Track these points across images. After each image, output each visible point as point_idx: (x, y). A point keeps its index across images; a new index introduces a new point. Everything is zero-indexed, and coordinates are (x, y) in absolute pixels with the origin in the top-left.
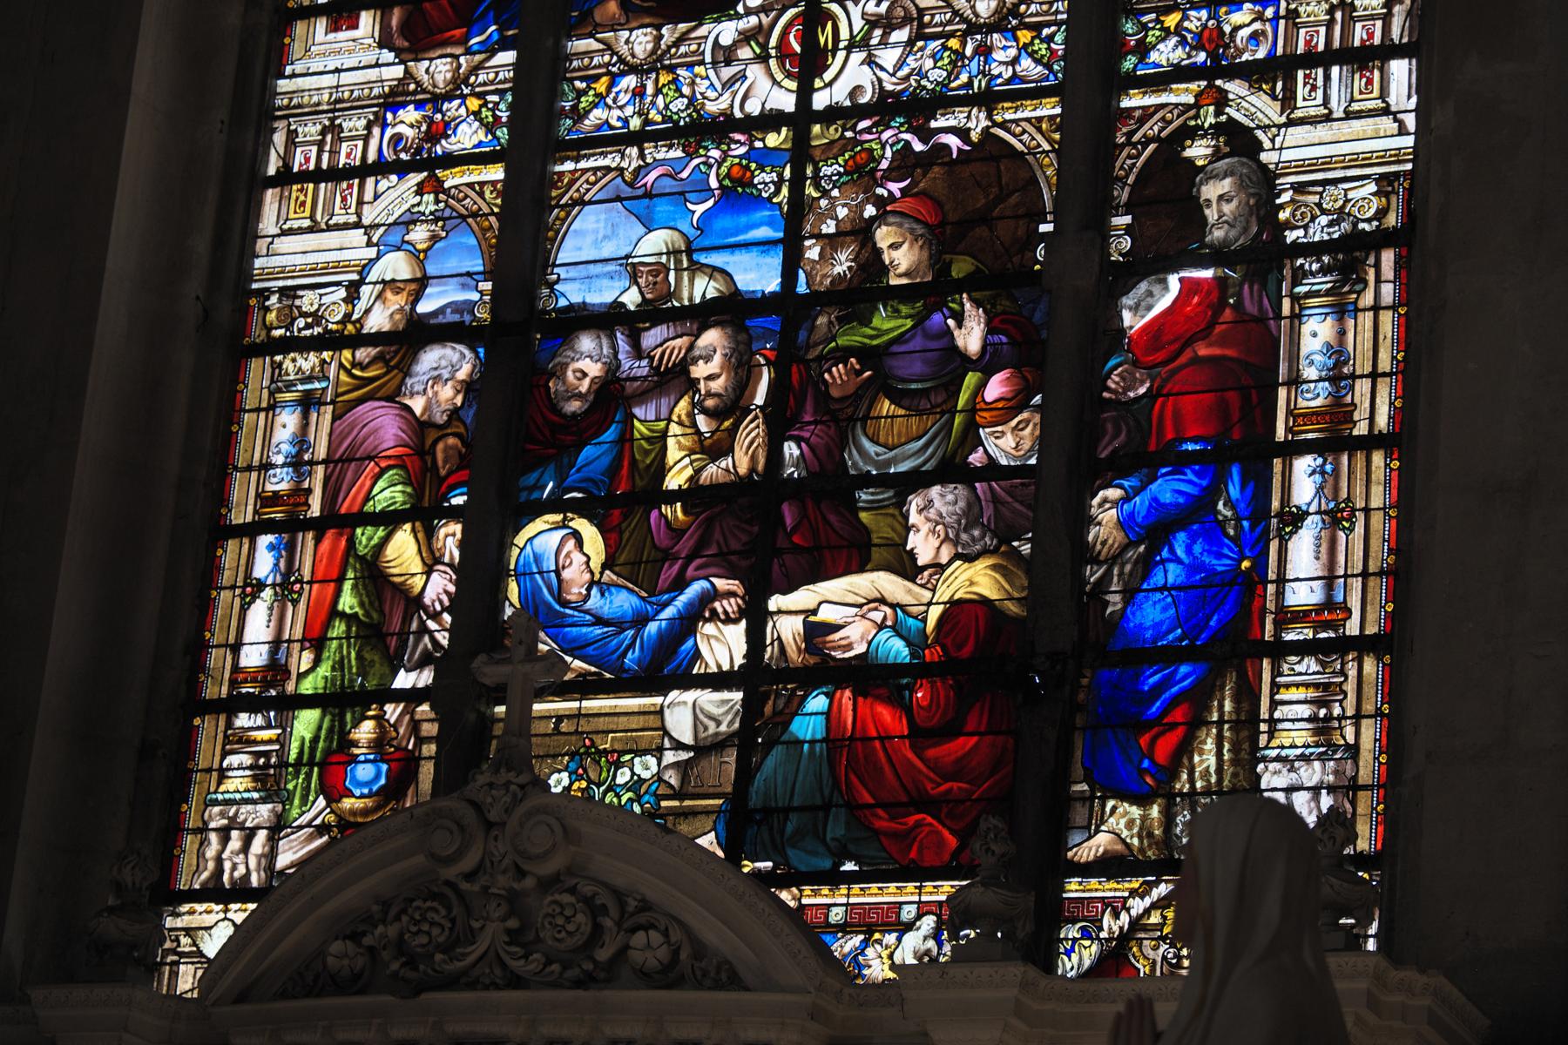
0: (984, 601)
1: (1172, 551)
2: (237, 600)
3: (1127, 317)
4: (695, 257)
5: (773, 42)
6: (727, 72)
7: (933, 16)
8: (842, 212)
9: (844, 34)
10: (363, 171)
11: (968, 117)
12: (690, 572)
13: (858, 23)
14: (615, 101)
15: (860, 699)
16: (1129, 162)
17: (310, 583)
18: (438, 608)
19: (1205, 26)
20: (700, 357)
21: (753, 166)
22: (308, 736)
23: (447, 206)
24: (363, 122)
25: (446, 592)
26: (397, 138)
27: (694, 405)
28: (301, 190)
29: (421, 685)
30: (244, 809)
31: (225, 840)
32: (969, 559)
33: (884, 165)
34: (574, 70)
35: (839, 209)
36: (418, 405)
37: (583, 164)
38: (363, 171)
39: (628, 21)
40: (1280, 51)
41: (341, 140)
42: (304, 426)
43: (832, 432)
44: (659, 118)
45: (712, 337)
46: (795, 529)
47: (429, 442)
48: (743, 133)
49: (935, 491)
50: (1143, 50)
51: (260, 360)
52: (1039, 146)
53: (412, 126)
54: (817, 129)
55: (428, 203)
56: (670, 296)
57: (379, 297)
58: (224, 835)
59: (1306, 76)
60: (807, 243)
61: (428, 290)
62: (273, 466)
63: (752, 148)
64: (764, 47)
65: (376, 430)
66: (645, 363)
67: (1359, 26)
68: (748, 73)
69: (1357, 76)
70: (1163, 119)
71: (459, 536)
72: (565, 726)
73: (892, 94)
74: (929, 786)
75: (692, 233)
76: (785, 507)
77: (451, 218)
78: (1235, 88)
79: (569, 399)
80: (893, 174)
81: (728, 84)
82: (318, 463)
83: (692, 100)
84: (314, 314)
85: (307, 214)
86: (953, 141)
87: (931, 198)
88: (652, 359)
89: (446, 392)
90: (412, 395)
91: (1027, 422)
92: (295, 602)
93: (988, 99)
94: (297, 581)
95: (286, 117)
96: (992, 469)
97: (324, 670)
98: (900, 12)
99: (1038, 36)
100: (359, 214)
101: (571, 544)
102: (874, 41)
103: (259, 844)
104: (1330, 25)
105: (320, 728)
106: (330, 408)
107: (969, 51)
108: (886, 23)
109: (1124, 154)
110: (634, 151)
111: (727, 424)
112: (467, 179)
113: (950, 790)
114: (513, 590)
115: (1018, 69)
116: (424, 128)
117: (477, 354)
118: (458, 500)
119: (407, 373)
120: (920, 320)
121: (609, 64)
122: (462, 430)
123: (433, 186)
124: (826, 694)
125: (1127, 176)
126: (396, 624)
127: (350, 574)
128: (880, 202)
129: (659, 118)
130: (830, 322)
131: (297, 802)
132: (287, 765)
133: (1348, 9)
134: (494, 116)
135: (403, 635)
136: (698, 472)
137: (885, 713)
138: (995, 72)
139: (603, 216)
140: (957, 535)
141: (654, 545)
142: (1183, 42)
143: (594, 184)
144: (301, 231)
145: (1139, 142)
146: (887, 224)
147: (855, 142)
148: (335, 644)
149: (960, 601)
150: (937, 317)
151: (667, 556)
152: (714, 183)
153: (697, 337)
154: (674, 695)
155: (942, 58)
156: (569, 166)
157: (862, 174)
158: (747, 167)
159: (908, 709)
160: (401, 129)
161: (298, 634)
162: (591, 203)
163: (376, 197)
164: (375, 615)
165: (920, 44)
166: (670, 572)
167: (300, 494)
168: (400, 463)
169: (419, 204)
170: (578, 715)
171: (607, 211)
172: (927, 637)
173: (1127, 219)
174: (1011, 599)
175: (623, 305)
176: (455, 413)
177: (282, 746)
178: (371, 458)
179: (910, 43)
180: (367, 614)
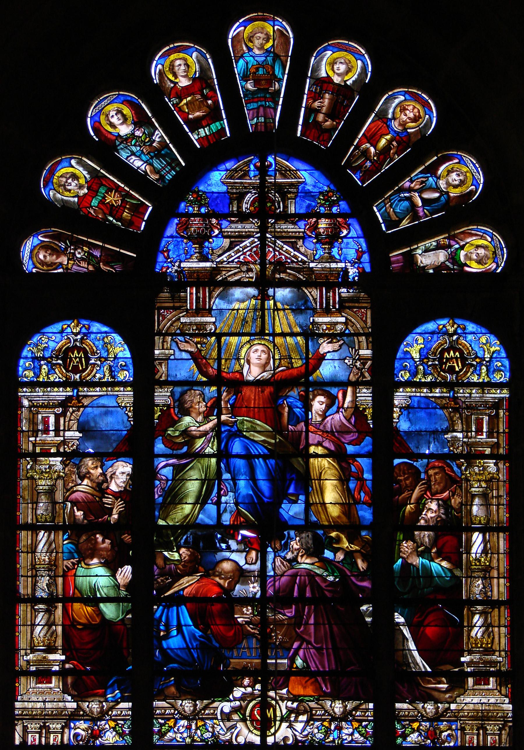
5: (248, 713)
7: (316, 711)
9: (278, 714)
13: (284, 711)
14: (178, 730)
19: (428, 729)
24: (59, 726)
26: (76, 735)
34: (158, 714)
39: (180, 697)
40: (459, 744)
41: (50, 733)
44: (198, 739)
50: (404, 736)
53: (84, 730)
64: (244, 715)
67: (489, 737)
68: (238, 725)
73: (301, 741)
81: (229, 729)
83: (213, 735)
95: (22, 719)
98: (302, 708)
99: (361, 725)
102: (292, 719)
104: (478, 735)
107: (333, 727)
108: (298, 712)
115: (354, 738)
116: (90, 732)
121: (174, 714)
134: (122, 730)
138: (344, 738)
142: (420, 735)
155: (321, 729)
179: (307, 722)
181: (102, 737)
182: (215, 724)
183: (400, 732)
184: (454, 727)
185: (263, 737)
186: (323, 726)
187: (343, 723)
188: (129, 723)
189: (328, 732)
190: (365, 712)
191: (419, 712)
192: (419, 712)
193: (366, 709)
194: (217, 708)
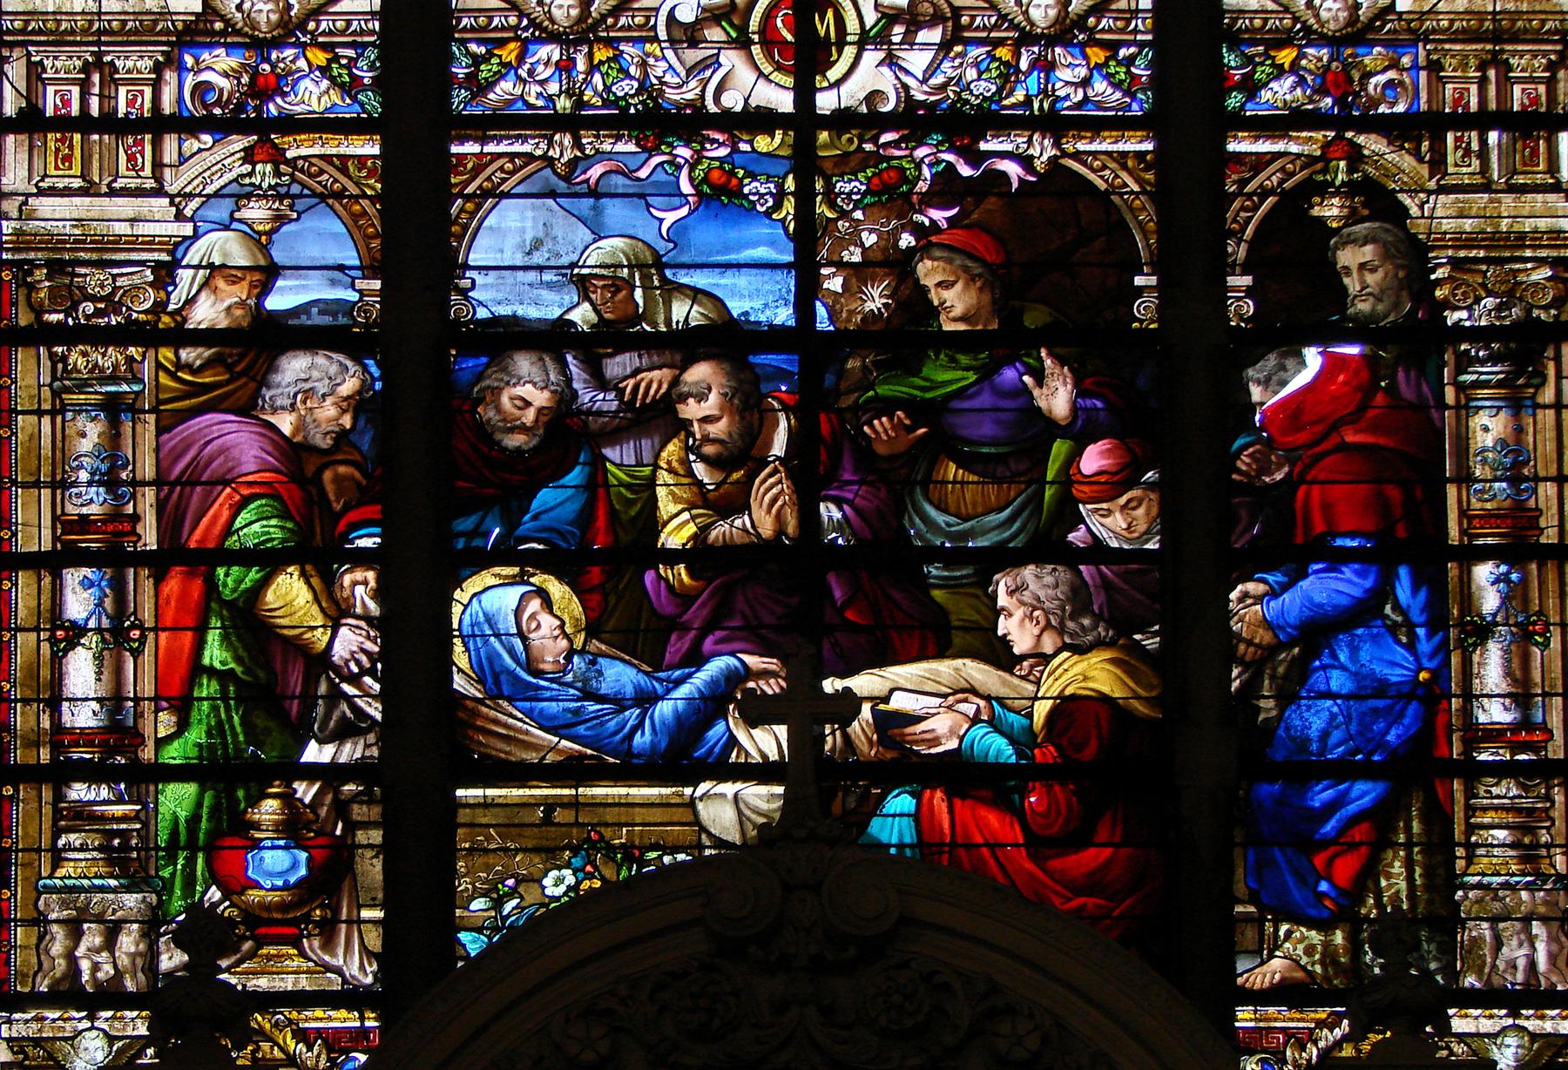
0: (1103, 698)
1: (1335, 657)
2: (45, 647)
3: (1256, 393)
4: (668, 273)
5: (754, 24)
6: (693, 56)
7: (973, 18)
8: (870, 239)
9: (852, 25)
10: (158, 124)
11: (1030, 142)
12: (708, 644)
13: (870, 18)
14: (531, 72)
15: (958, 803)
16: (1243, 214)
17: (156, 629)
18: (355, 669)
19: (1327, 68)
20: (690, 395)
21: (741, 173)
22: (183, 814)
23: (294, 180)
25: (363, 650)
27: (688, 449)
28: (62, 141)
29: (343, 759)
30: (97, 897)
31: (76, 934)
32: (1079, 650)
33: (922, 187)
34: (465, 30)
35: (864, 235)
36: (286, 423)
37: (491, 148)
38: (158, 124)
42: (113, 438)
43: (883, 494)
44: (597, 101)
45: (700, 372)
46: (847, 603)
47: (310, 470)
48: (721, 131)
49: (1029, 572)
50: (1251, 88)
51: (32, 351)
52: (1126, 185)
53: (226, 75)
54: (824, 136)
55: (264, 174)
56: (637, 318)
57: (206, 284)
58: (75, 929)
59: (1457, 139)
60: (824, 271)
61: (279, 283)
62: (75, 484)
63: (735, 150)
64: (743, 29)
65: (223, 451)
66: (611, 396)
68: (722, 59)
69: (1519, 145)
70: (1282, 169)
71: (372, 584)
72: (559, 815)
74: (1057, 901)
75: (662, 247)
76: (832, 579)
77: (301, 196)
78: (1372, 144)
79: (512, 430)
80: (935, 198)
82: (144, 484)
84: (108, 299)
85: (76, 170)
86: (1012, 169)
87: (989, 232)
88: (621, 392)
89: (328, 411)
90: (275, 410)
91: (1140, 502)
92: (137, 654)
93: (1054, 124)
94: (133, 627)
96: (1097, 551)
97: (196, 734)
98: (926, 8)
99: (1114, 56)
100: (159, 179)
101: (535, 605)
103: (128, 942)
105: (199, 805)
106: (151, 418)
107: (1024, 65)
108: (913, 20)
109: (1236, 205)
110: (568, 140)
111: (735, 476)
112: (316, 150)
113: (1083, 907)
114: (460, 657)
115: (1090, 93)
116: (245, 79)
117: (365, 369)
118: (367, 542)
119: (264, 382)
120: (987, 373)
121: (516, 28)
122: (356, 457)
123: (264, 151)
124: (912, 794)
125: (1243, 230)
126: (296, 682)
127: (215, 622)
128: (918, 230)
129: (597, 101)
130: (864, 366)
131: (178, 892)
132: (157, 848)
133: (1503, 69)
134: (351, 74)
135: (309, 700)
136: (704, 530)
137: (992, 819)
138: (1061, 93)
139: (529, 214)
140: (1062, 623)
141: (654, 612)
142: (1301, 82)
143: (513, 173)
144: (67, 192)
145: (1254, 193)
146: (930, 258)
147: (876, 158)
148: (205, 705)
149: (1074, 697)
150: (1009, 374)
151: (673, 625)
152: (686, 188)
153: (684, 369)
154: (703, 787)
155: (988, 69)
156: (471, 148)
157: (892, 195)
158: (732, 173)
159: (1019, 814)
160: (207, 76)
161: (148, 690)
162: (508, 195)
163: (183, 160)
164: (261, 674)
165: (958, 49)
166: (677, 645)
167: (121, 522)
168: (269, 491)
169: (250, 175)
170: (575, 804)
171: (534, 208)
172: (1035, 736)
173: (1247, 280)
174: (1137, 697)
175: (573, 324)
176: (342, 437)
177: (145, 825)
178: (226, 483)
179: (945, 47)
180: (247, 671)
181: (284, 95)
182: (648, 55)
183: (1237, 74)
184: (1406, 61)
185: (805, 94)
186: (994, 59)
187: (1058, 50)
188: (372, 54)
189: (1009, 75)
190: (1128, 21)
191: (1296, 20)
192: (1296, 20)
193: (1129, 11)
194: (657, 10)
